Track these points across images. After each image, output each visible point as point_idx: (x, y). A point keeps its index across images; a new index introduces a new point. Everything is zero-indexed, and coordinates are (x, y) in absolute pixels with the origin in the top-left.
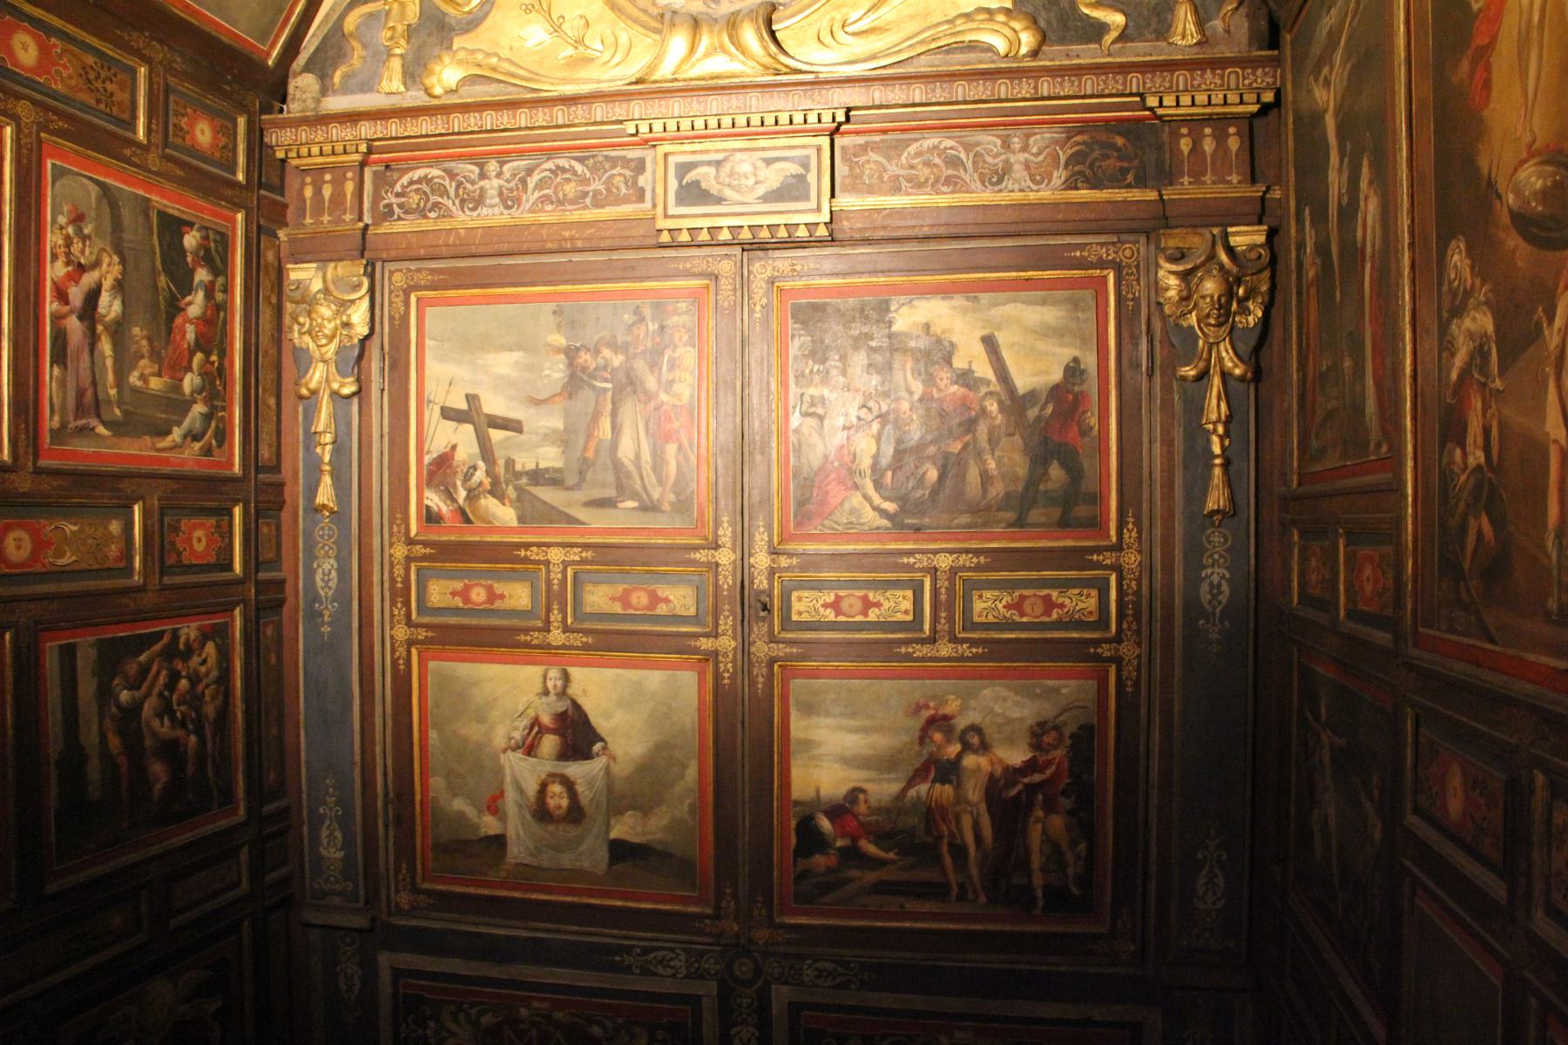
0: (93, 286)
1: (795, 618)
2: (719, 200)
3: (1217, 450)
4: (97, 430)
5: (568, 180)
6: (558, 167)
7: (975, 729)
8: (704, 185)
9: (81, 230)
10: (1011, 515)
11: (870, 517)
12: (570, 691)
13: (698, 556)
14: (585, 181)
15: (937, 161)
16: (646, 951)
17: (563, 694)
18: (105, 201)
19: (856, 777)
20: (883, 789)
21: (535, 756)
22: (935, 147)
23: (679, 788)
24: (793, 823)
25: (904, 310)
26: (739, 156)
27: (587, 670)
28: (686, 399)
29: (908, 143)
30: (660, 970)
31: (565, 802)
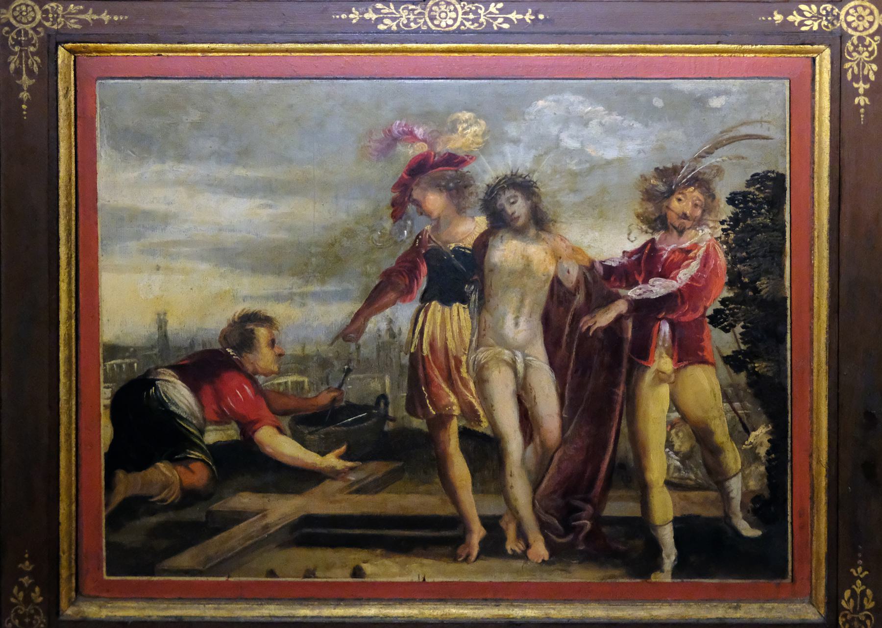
24: (106, 395)
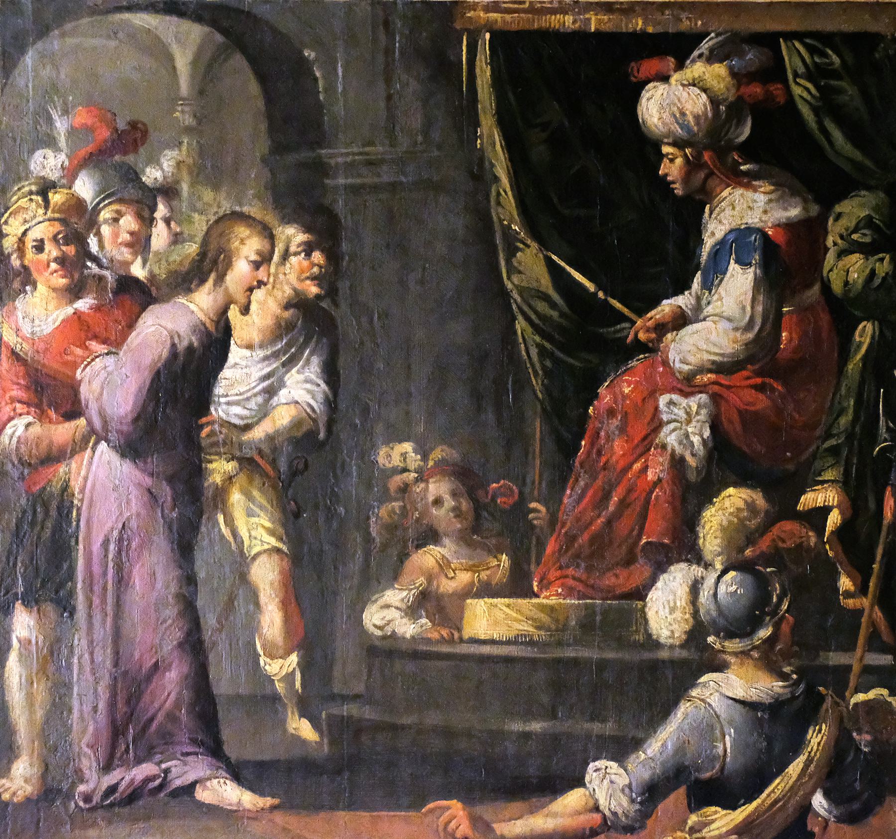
0: (187, 338)
4: (203, 795)
9: (132, 176)
18: (238, 61)
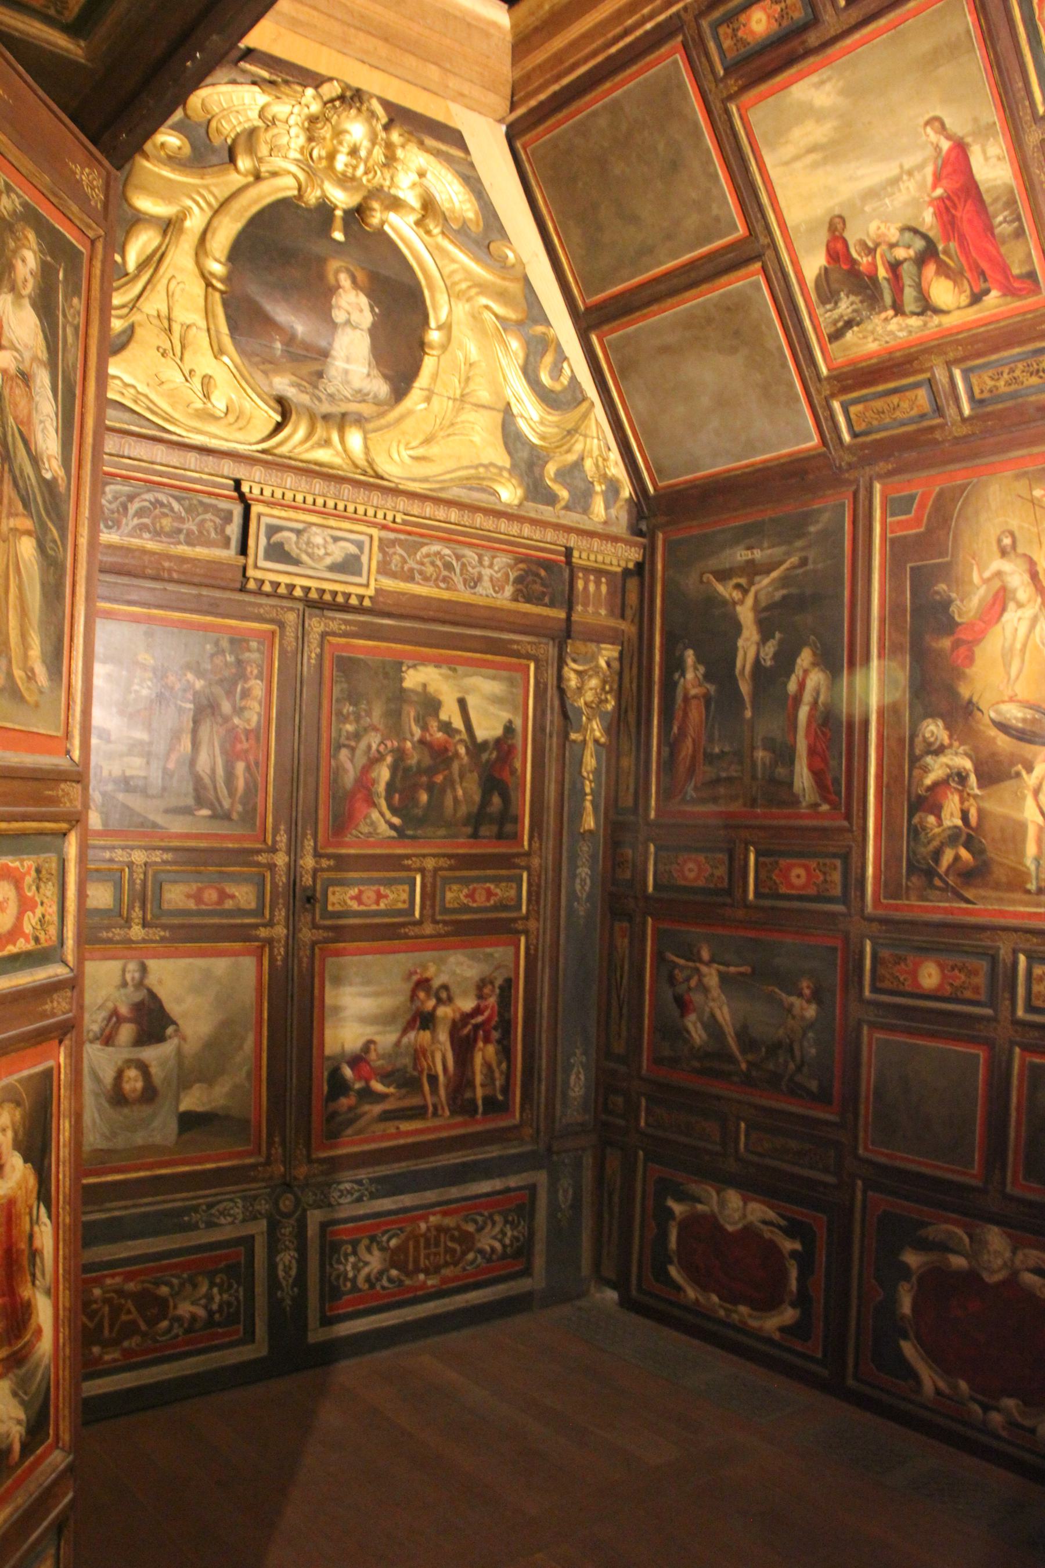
1: (330, 908)
2: (297, 562)
3: (588, 790)
5: (165, 515)
6: (157, 501)
7: (445, 987)
8: (287, 548)
10: (469, 830)
11: (383, 829)
12: (147, 982)
13: (260, 858)
14: (182, 520)
15: (439, 563)
16: (210, 1206)
17: (140, 984)
19: (368, 1032)
20: (387, 1039)
21: (113, 1045)
22: (439, 553)
23: (238, 1059)
24: (326, 1074)
25: (411, 672)
26: (314, 529)
27: (163, 962)
28: (254, 723)
29: (423, 545)
30: (222, 1221)
31: (139, 1085)
